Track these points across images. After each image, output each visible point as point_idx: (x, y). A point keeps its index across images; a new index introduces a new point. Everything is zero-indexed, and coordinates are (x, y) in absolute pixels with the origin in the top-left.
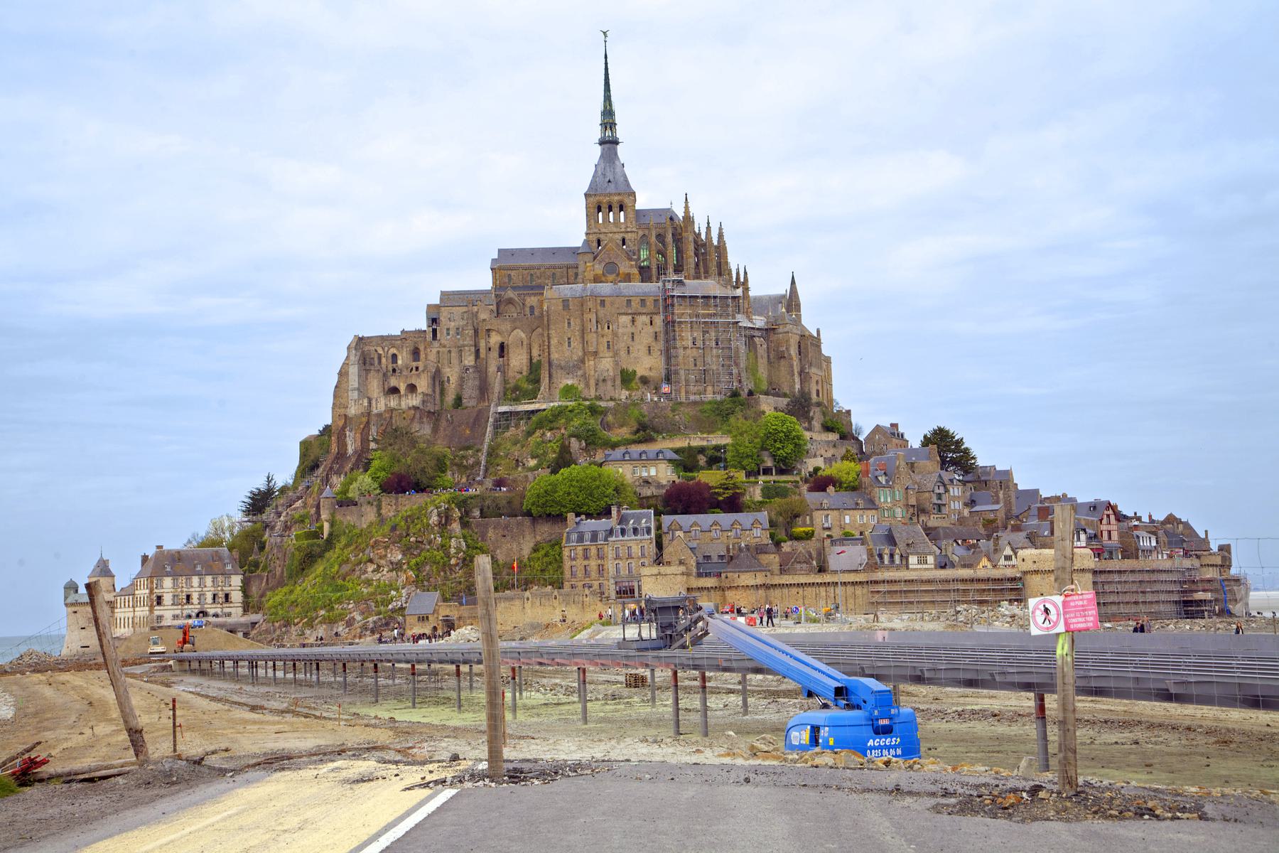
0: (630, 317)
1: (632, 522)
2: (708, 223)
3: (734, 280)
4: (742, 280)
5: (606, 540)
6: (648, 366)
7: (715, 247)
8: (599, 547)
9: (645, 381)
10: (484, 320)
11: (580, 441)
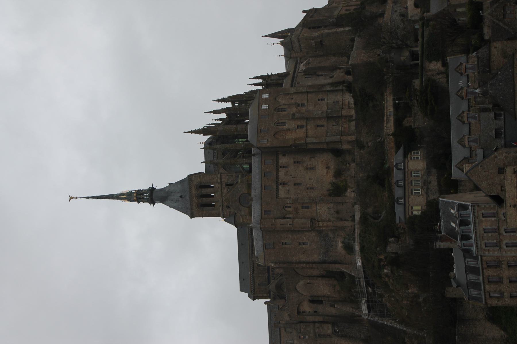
0: (280, 187)
1: (454, 225)
2: (210, 112)
3: (260, 88)
4: (261, 81)
5: (476, 258)
6: (325, 171)
7: (233, 104)
8: (485, 266)
9: (338, 174)
10: (290, 316)
11: (390, 242)
